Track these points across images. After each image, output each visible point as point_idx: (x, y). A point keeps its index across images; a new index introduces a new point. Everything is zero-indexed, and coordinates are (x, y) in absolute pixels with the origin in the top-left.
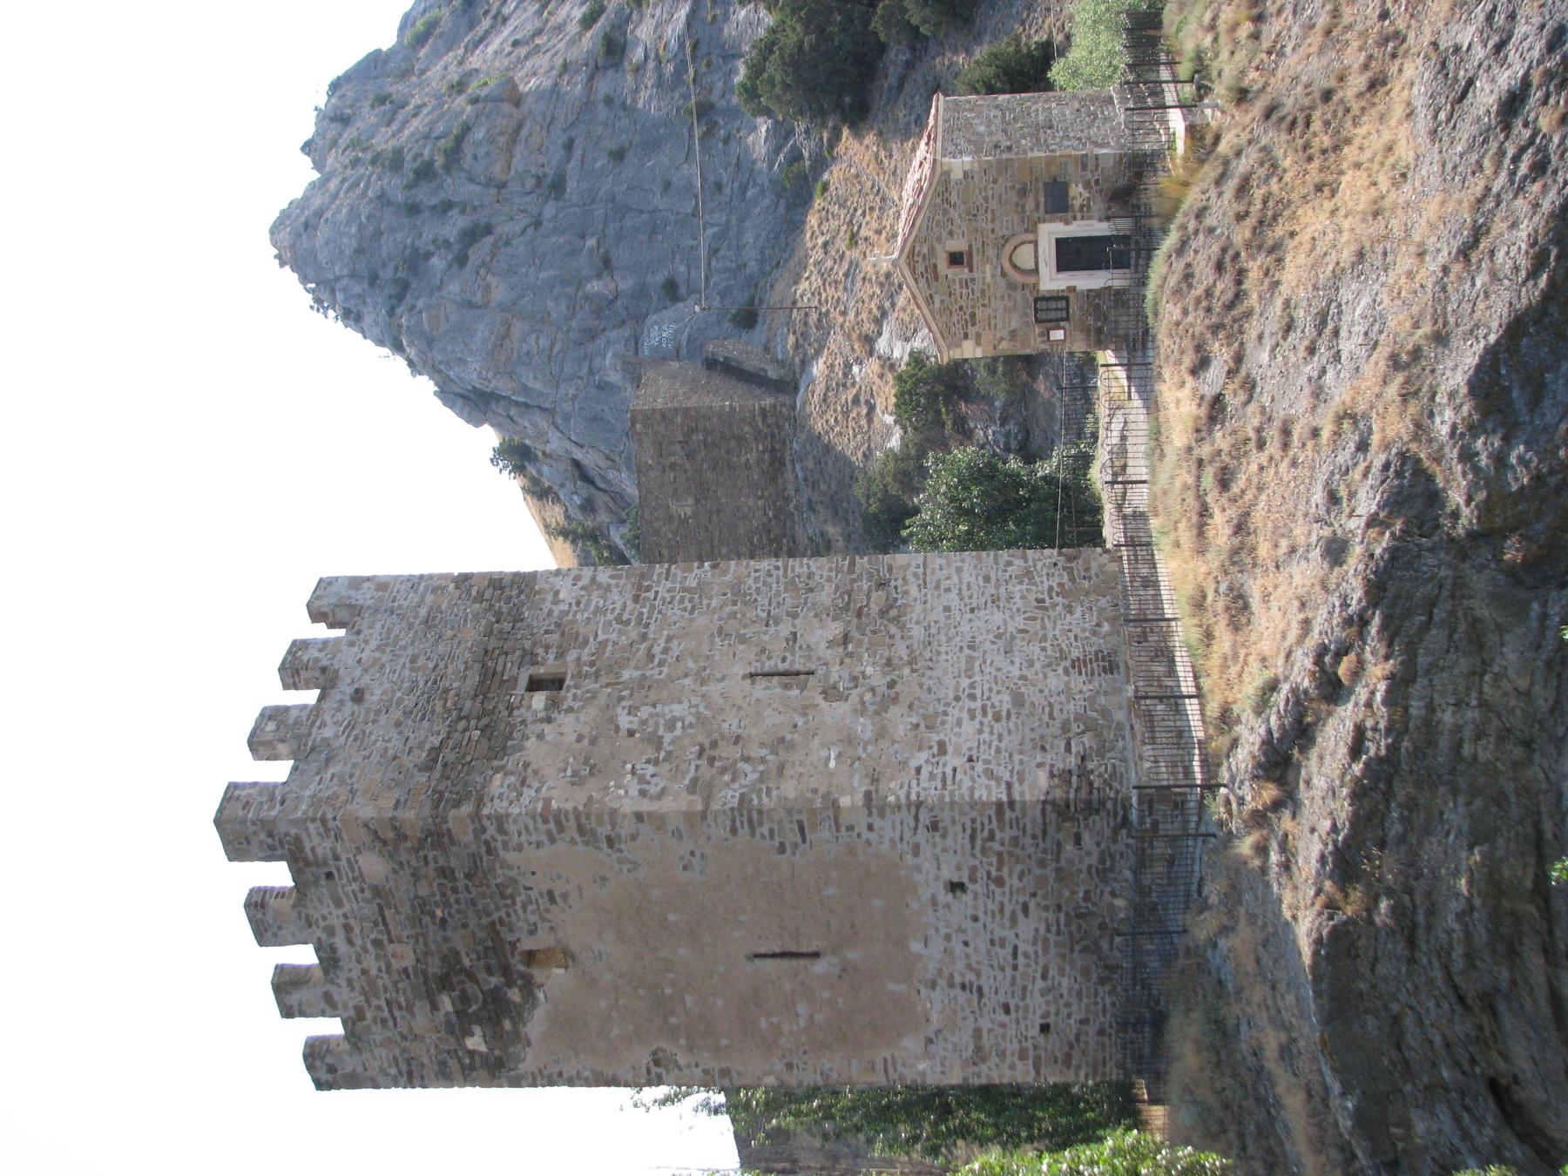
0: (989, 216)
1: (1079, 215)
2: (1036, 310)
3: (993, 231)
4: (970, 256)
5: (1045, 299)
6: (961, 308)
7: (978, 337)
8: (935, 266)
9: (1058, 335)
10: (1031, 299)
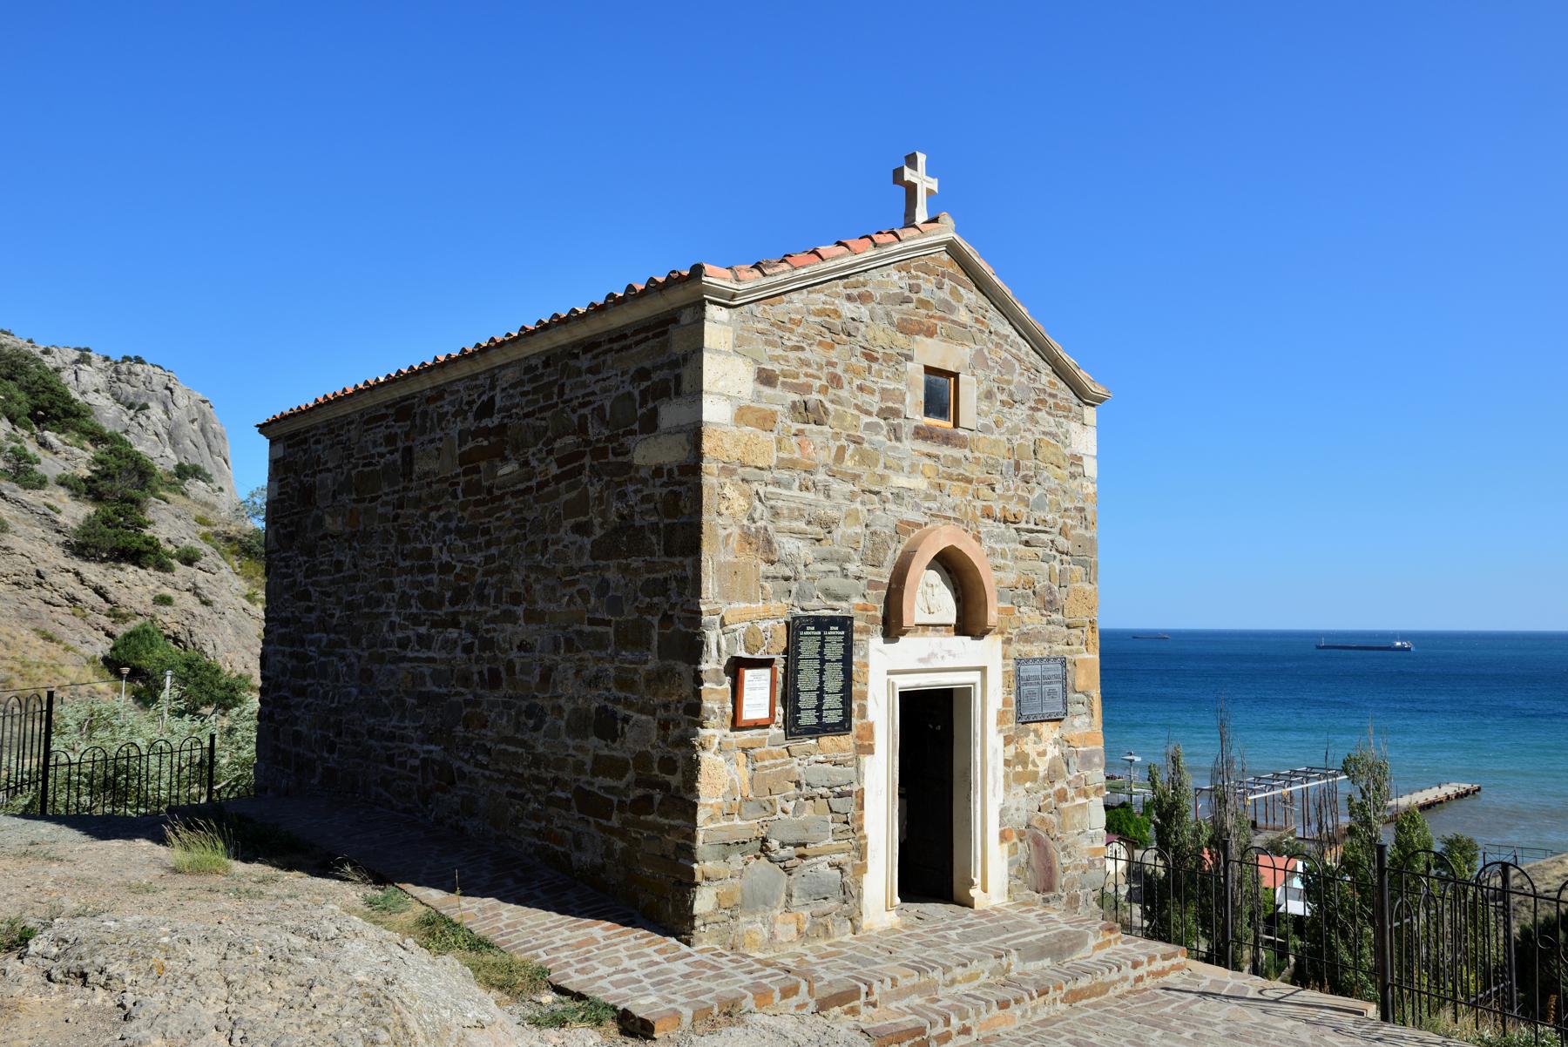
0: (1014, 507)
1: (1012, 749)
2: (821, 624)
3: (988, 514)
4: (947, 439)
5: (847, 660)
6: (835, 381)
7: (766, 421)
8: (930, 333)
9: (758, 691)
10: (843, 609)
